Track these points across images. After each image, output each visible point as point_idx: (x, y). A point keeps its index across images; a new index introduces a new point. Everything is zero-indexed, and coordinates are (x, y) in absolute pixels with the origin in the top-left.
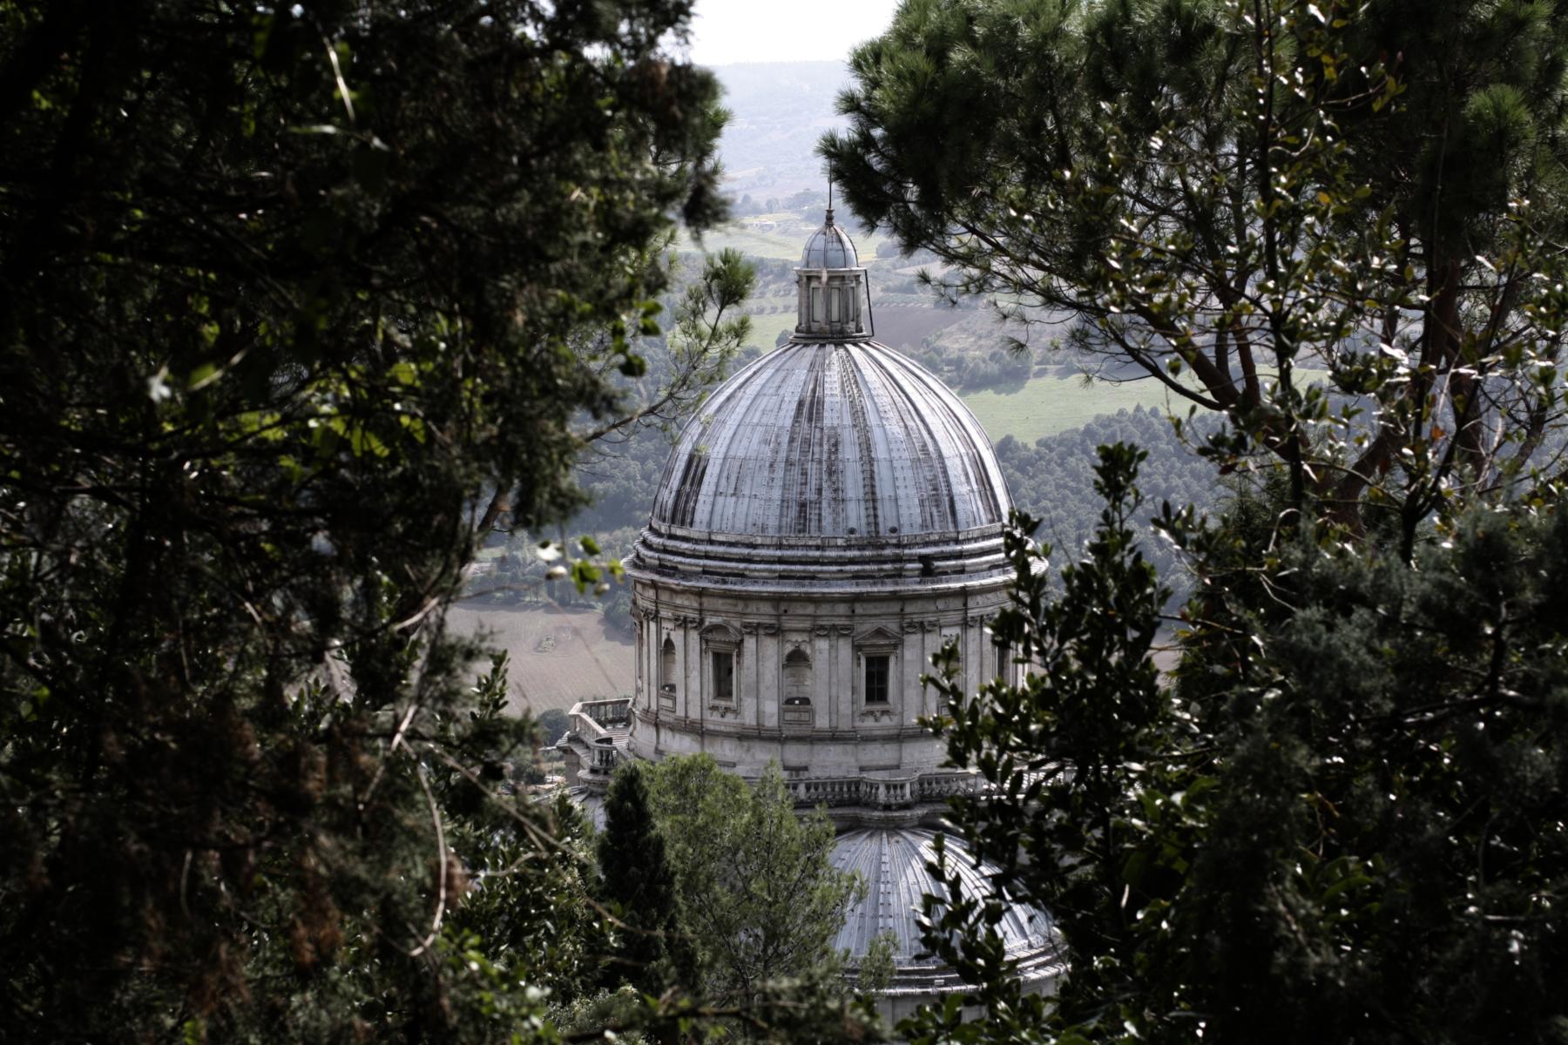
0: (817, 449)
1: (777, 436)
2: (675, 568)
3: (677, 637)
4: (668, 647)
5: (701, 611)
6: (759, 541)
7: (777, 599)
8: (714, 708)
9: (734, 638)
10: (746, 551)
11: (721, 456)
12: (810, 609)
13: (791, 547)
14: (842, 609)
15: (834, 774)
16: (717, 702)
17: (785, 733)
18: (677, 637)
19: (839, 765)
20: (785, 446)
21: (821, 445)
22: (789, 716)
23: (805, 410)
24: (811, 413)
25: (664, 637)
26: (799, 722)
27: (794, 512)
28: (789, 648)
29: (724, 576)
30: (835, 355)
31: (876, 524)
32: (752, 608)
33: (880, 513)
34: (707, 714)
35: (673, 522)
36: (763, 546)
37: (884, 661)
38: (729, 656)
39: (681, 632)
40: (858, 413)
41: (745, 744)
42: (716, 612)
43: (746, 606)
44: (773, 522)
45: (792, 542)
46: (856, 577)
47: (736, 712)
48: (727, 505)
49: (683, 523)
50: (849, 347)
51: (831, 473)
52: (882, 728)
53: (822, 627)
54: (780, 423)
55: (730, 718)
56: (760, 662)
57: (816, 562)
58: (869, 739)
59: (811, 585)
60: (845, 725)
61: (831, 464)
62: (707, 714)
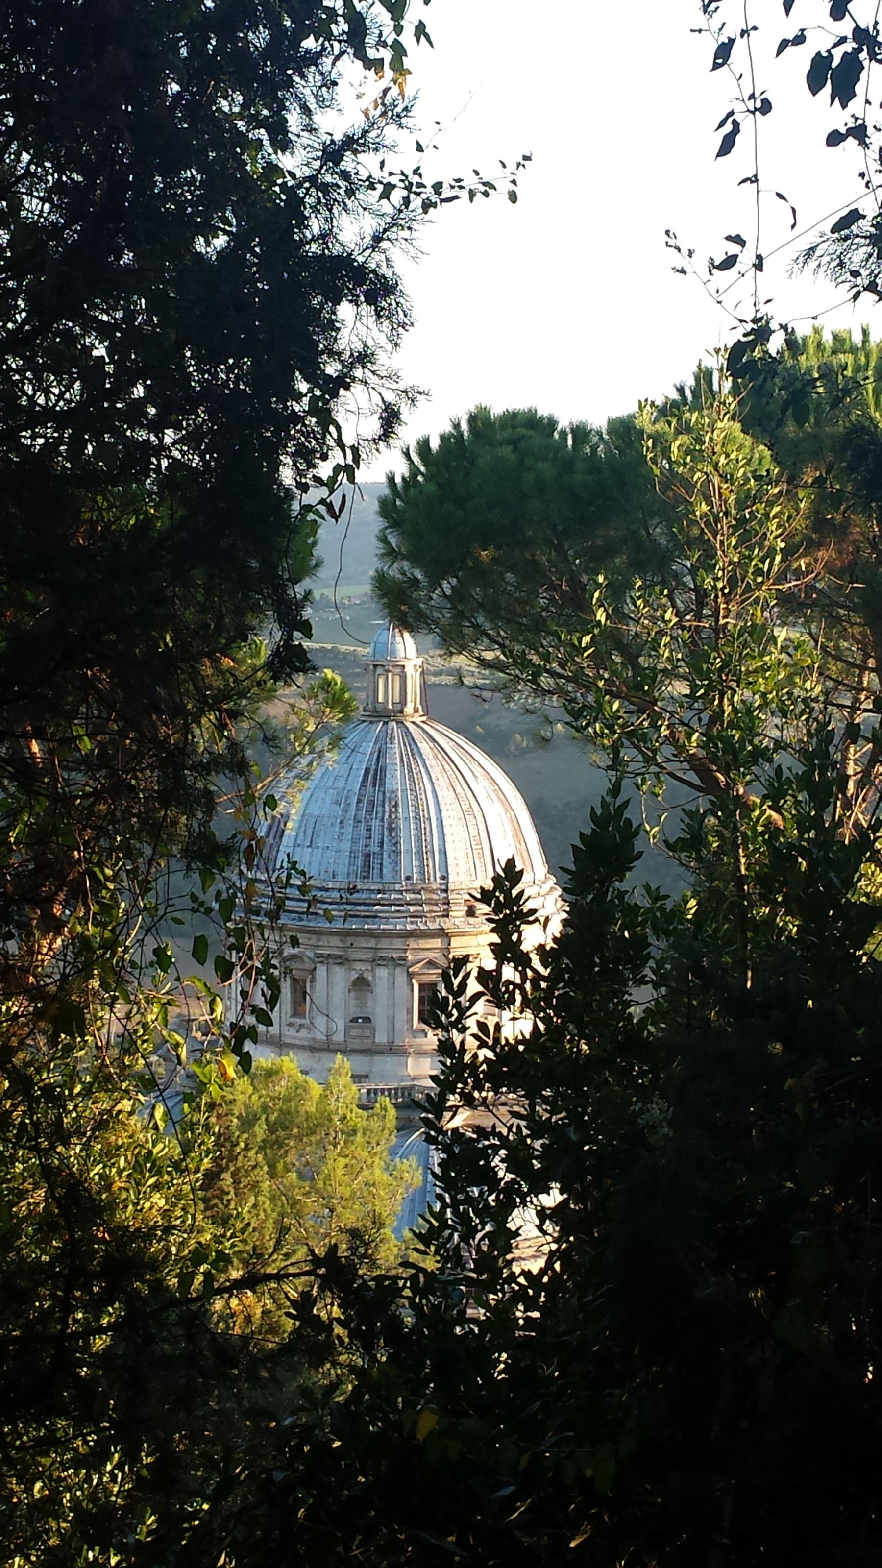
0: (380, 809)
1: (347, 798)
8: (291, 1025)
9: (308, 965)
12: (372, 943)
16: (293, 1020)
21: (384, 806)
22: (354, 1033)
27: (360, 861)
28: (354, 975)
32: (324, 941)
38: (305, 981)
41: (317, 1055)
43: (319, 940)
44: (342, 869)
51: (391, 830)
53: (382, 958)
54: (348, 788)
55: (304, 1033)
61: (390, 825)
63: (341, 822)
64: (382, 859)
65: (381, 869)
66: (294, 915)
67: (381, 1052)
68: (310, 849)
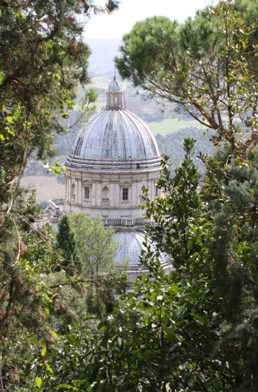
0: (111, 136)
2: (75, 166)
3: (76, 183)
4: (73, 185)
5: (82, 176)
6: (96, 159)
7: (101, 174)
8: (85, 201)
10: (93, 162)
12: (109, 176)
13: (104, 161)
14: (117, 176)
16: (86, 200)
18: (76, 183)
22: (103, 203)
23: (108, 127)
27: (105, 152)
28: (103, 186)
29: (88, 168)
30: (116, 113)
31: (126, 155)
32: (94, 176)
33: (126, 152)
36: (97, 160)
40: (121, 128)
41: (93, 210)
42: (86, 177)
46: (121, 168)
47: (90, 202)
49: (77, 154)
50: (119, 111)
51: (114, 142)
53: (112, 181)
55: (89, 203)
56: (97, 189)
57: (111, 165)
58: (123, 209)
60: (117, 205)
61: (114, 140)
62: (83, 202)
65: (112, 154)
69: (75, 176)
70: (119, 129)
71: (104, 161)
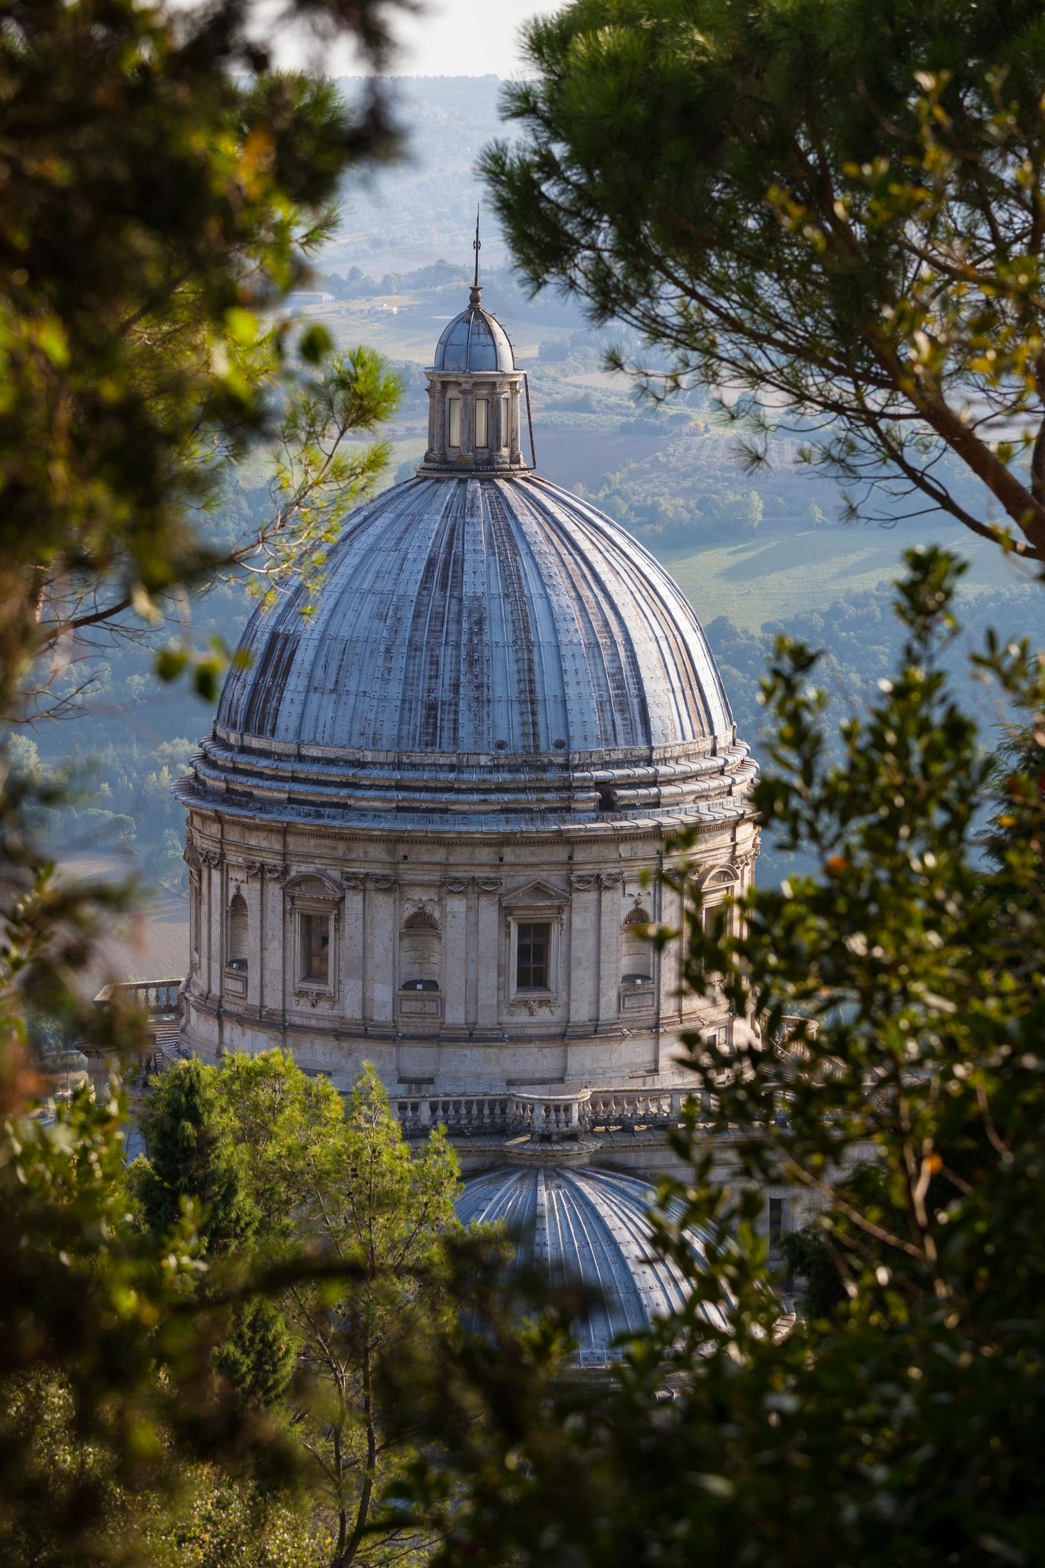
0: (453, 628)
1: (397, 608)
2: (250, 795)
3: (251, 892)
5: (284, 855)
6: (369, 756)
8: (301, 994)
9: (333, 894)
11: (316, 635)
12: (440, 854)
13: (414, 766)
14: (485, 854)
15: (469, 1089)
16: (306, 986)
17: (403, 1030)
19: (479, 1076)
20: (408, 623)
21: (459, 622)
22: (407, 1006)
24: (445, 577)
25: (232, 892)
26: (423, 1015)
27: (419, 717)
28: (409, 910)
29: (319, 807)
31: (535, 735)
32: (359, 851)
33: (541, 719)
34: (292, 1004)
35: (247, 728)
37: (543, 930)
39: (257, 885)
41: (345, 1045)
42: (307, 857)
43: (349, 849)
44: (389, 730)
45: (416, 759)
48: (323, 706)
49: (260, 732)
51: (472, 662)
52: (540, 1025)
53: (457, 881)
54: (401, 591)
55: (324, 1008)
57: (449, 789)
58: (520, 1039)
59: (443, 822)
60: (486, 1020)
62: (292, 1004)
63: (388, 650)
64: (456, 712)
65: (455, 730)
66: (307, 809)
67: (454, 1040)
68: (334, 697)
69: (250, 849)
70: (497, 587)
71: (414, 766)
